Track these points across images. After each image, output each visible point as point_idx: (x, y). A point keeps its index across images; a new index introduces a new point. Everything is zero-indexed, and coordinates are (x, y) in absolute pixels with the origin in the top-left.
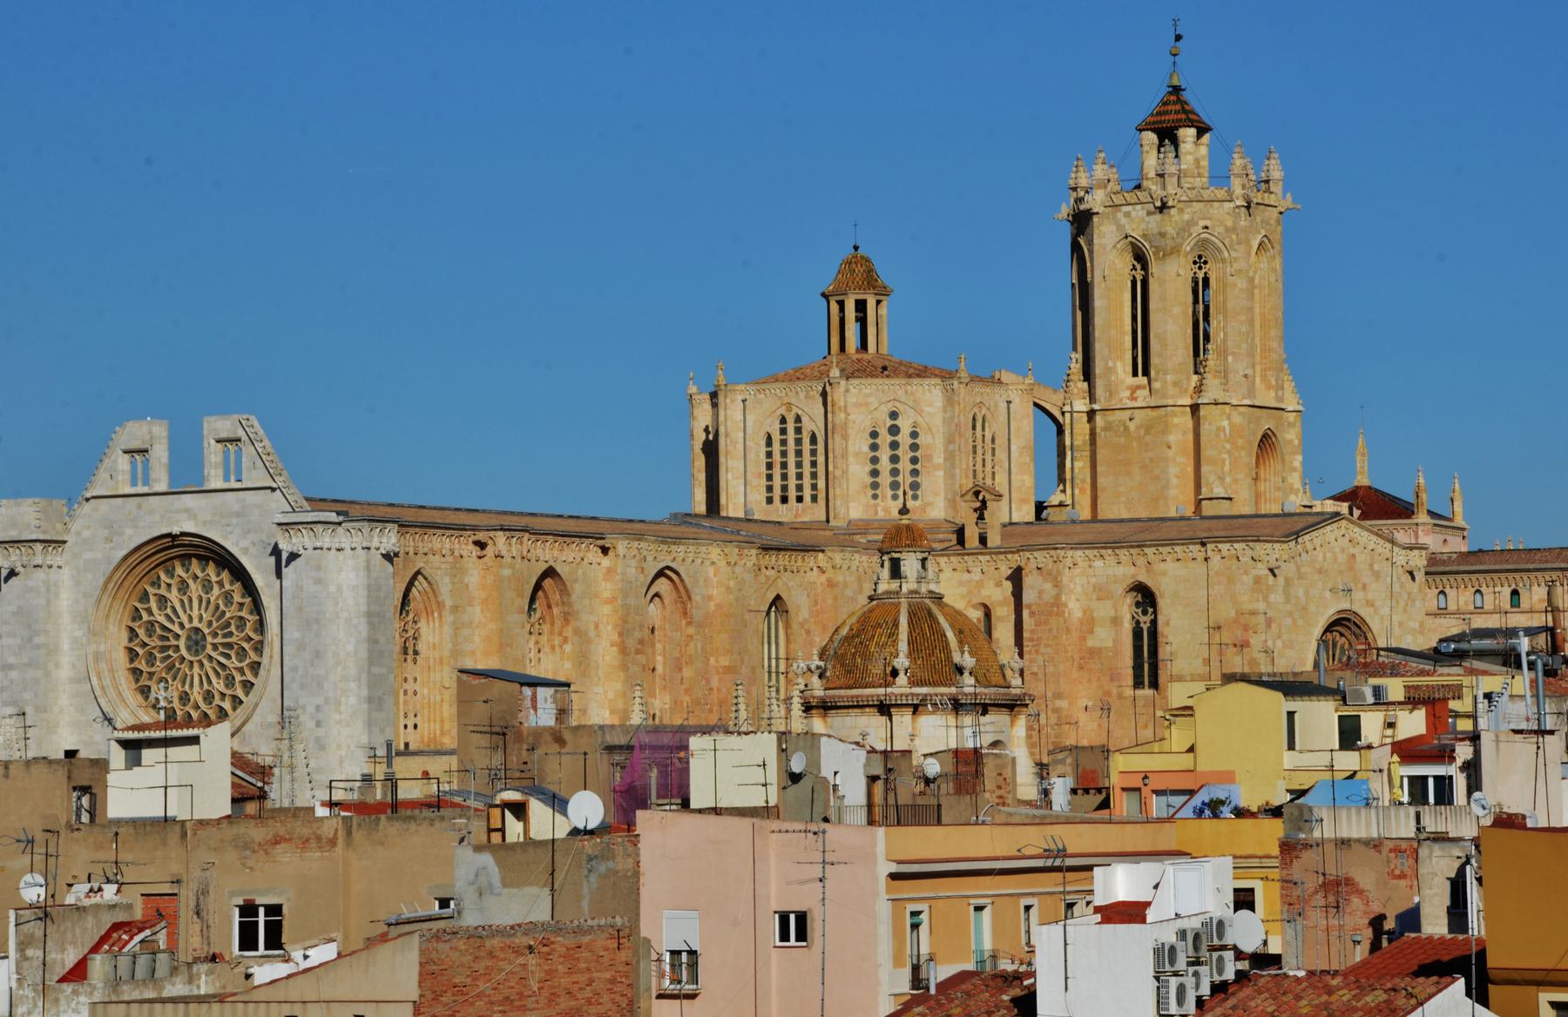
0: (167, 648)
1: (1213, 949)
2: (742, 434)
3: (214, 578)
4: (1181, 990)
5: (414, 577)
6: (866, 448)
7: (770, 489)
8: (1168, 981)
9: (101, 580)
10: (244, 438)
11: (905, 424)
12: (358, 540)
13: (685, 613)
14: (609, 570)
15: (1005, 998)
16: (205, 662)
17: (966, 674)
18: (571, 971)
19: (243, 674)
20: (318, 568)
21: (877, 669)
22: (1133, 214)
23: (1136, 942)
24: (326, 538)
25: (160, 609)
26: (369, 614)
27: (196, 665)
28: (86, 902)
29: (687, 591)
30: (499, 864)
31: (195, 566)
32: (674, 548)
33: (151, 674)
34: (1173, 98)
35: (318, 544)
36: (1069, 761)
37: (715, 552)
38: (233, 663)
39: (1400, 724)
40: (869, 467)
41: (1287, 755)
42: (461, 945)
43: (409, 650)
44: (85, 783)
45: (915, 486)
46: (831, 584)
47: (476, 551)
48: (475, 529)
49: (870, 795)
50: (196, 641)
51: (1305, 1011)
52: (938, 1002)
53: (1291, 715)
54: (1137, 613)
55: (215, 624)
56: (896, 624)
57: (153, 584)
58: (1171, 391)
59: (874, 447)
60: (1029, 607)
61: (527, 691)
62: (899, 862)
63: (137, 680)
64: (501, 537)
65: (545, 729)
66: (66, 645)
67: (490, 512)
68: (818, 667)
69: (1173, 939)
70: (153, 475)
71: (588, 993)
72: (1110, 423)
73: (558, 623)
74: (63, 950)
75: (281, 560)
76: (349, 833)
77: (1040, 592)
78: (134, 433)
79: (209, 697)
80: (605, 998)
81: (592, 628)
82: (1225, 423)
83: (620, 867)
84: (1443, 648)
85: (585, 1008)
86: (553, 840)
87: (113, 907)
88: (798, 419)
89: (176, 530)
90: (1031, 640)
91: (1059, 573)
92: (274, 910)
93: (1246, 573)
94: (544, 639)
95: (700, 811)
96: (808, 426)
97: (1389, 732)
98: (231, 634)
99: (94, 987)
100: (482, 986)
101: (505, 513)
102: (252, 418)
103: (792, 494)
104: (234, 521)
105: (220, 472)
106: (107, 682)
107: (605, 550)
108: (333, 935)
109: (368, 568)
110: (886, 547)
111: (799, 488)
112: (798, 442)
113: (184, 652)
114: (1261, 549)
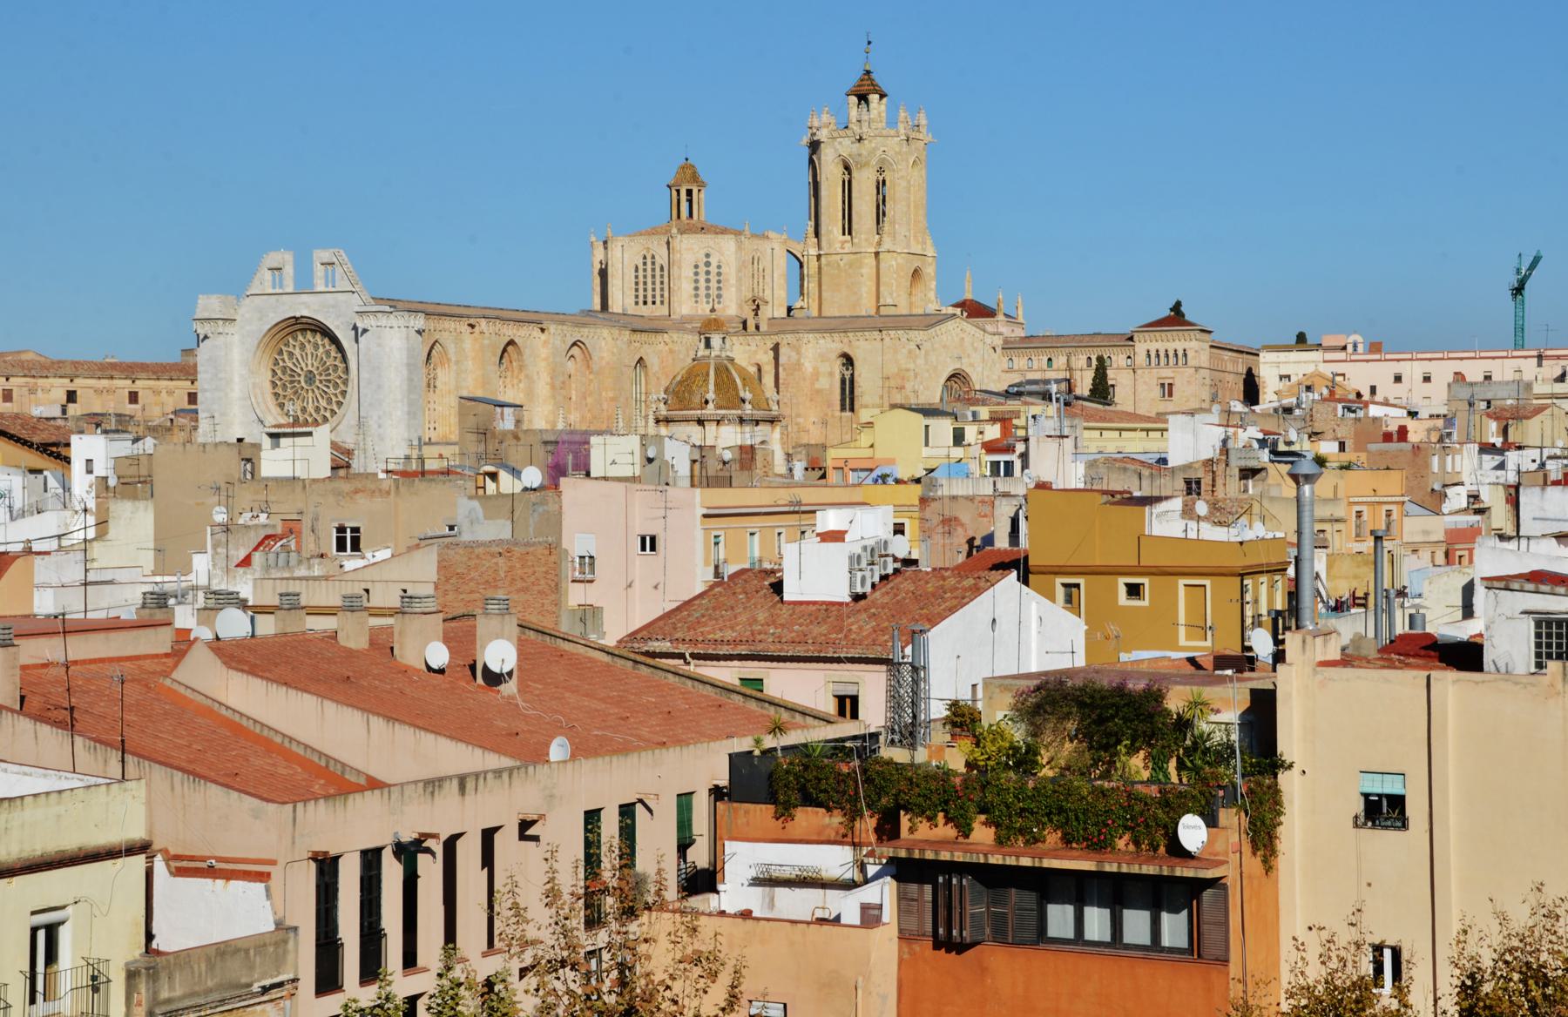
0: (294, 381)
1: (881, 556)
3: (320, 343)
4: (863, 580)
5: (434, 344)
6: (692, 274)
7: (637, 297)
9: (256, 342)
10: (337, 262)
11: (714, 261)
12: (402, 322)
13: (588, 367)
14: (545, 342)
15: (766, 583)
17: (747, 403)
20: (379, 338)
21: (697, 400)
23: (838, 555)
24: (383, 320)
26: (408, 365)
28: (250, 523)
29: (590, 355)
30: (481, 504)
32: (582, 329)
33: (285, 396)
34: (866, 77)
37: (605, 332)
38: (331, 391)
39: (986, 432)
40: (693, 285)
42: (461, 551)
43: (431, 385)
44: (248, 457)
45: (719, 296)
46: (671, 351)
48: (469, 317)
49: (692, 470)
50: (310, 378)
51: (930, 590)
52: (729, 585)
53: (927, 427)
55: (321, 369)
56: (708, 375)
57: (285, 345)
58: (864, 244)
59: (696, 274)
61: (498, 410)
62: (708, 508)
64: (483, 322)
65: (508, 431)
66: (236, 379)
67: (477, 307)
69: (859, 551)
70: (285, 283)
71: (532, 579)
74: (237, 549)
75: (358, 332)
76: (397, 488)
77: (789, 357)
78: (273, 259)
79: (317, 409)
80: (542, 582)
82: (894, 263)
84: (1011, 390)
87: (266, 526)
88: (653, 257)
89: (298, 315)
91: (800, 346)
92: (356, 530)
94: (508, 380)
95: (596, 478)
96: (659, 261)
97: (980, 436)
98: (330, 374)
99: (255, 570)
100: (473, 574)
101: (486, 308)
102: (342, 252)
103: (650, 300)
105: (323, 281)
106: (260, 400)
107: (543, 330)
109: (407, 338)
110: (703, 331)
111: (654, 296)
112: (653, 270)
113: (303, 384)
114: (912, 334)
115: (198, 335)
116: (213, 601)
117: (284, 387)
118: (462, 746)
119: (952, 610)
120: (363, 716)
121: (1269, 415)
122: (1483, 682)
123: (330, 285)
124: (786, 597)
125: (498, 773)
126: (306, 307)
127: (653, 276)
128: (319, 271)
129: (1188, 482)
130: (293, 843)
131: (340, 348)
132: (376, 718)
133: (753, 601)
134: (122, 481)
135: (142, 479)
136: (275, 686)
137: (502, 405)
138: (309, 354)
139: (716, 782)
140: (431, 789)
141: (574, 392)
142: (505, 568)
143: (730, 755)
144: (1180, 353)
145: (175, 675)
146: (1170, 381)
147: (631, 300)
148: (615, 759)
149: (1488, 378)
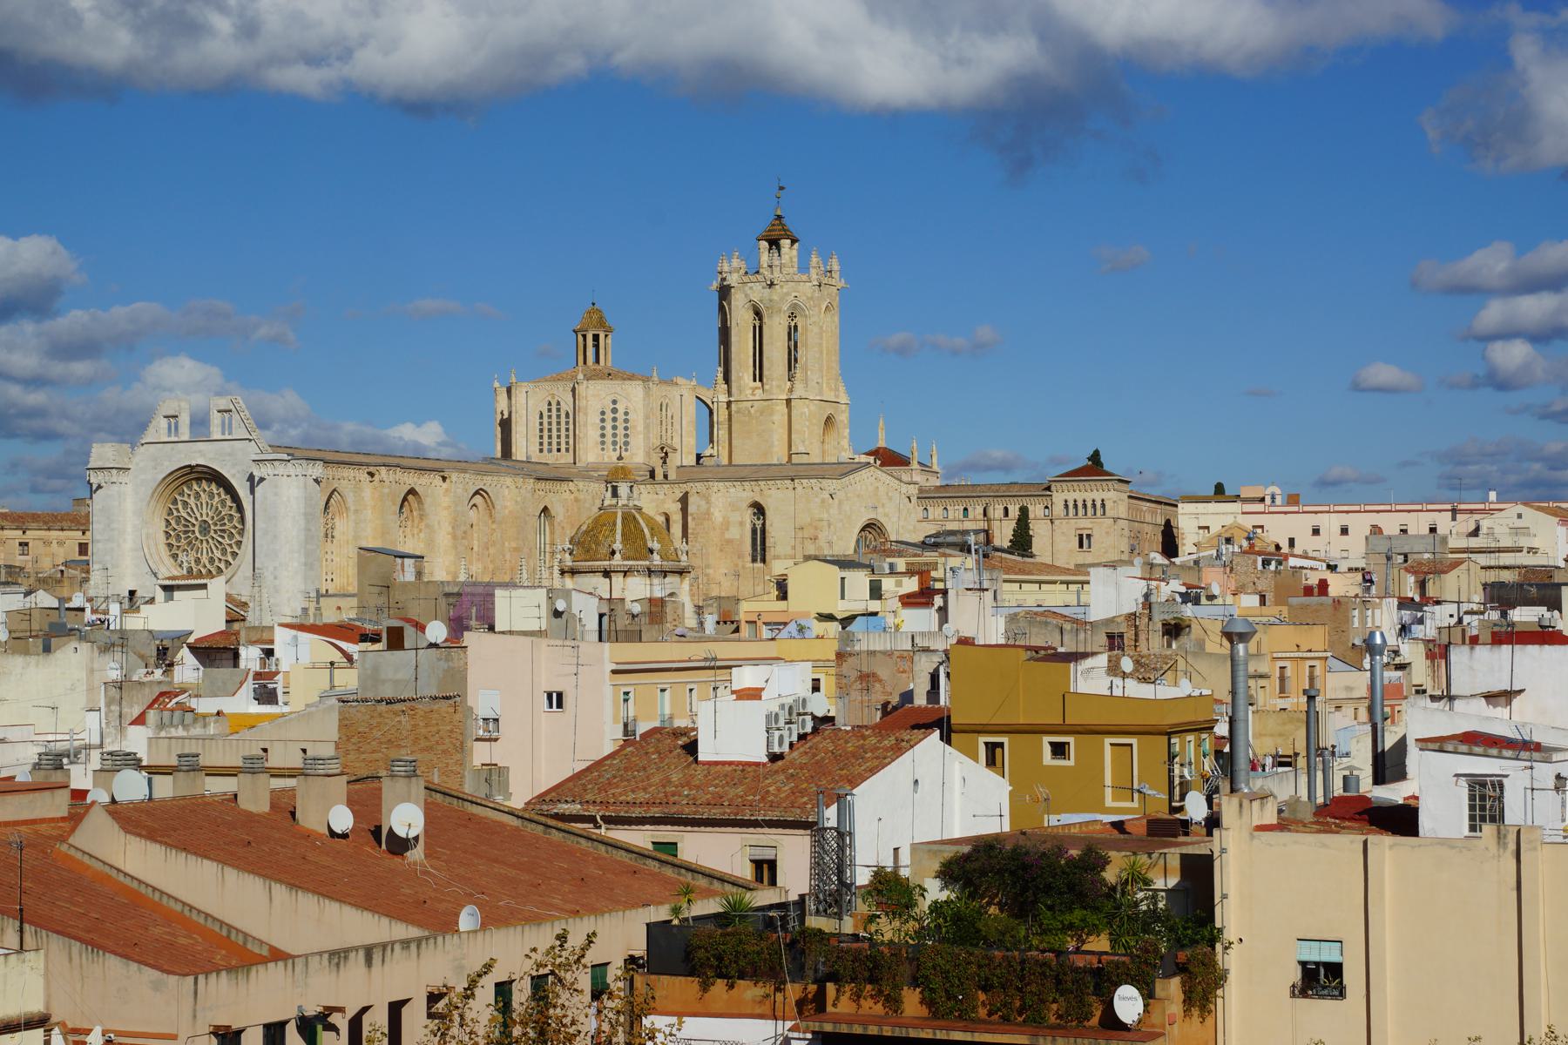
0: (188, 532)
1: (799, 714)
3: (215, 492)
4: (781, 738)
5: (332, 493)
6: (598, 421)
9: (150, 492)
10: (234, 409)
11: (621, 407)
12: (299, 470)
14: (447, 490)
16: (210, 540)
17: (655, 554)
18: (427, 725)
19: (232, 548)
23: (755, 713)
24: (281, 469)
26: (305, 514)
28: (145, 680)
31: (204, 485)
32: (485, 478)
35: (276, 473)
36: (715, 605)
37: (509, 481)
38: (226, 541)
40: (600, 432)
41: (840, 602)
43: (329, 535)
45: (626, 443)
46: (577, 500)
47: (368, 478)
48: (368, 465)
50: (205, 527)
53: (843, 579)
57: (180, 494)
58: (775, 391)
59: (603, 420)
60: (692, 515)
61: (399, 561)
62: (617, 663)
66: (129, 529)
69: (777, 709)
70: (180, 431)
73: (416, 521)
74: (132, 707)
77: (699, 506)
79: (212, 561)
81: (436, 523)
83: (456, 665)
87: (160, 683)
88: (558, 403)
89: (194, 463)
90: (693, 534)
94: (408, 530)
95: (503, 633)
96: (564, 407)
98: (225, 524)
102: (239, 398)
104: (228, 458)
105: (220, 429)
107: (444, 479)
109: (305, 487)
110: (609, 479)
111: (559, 444)
112: (558, 417)
113: (197, 534)
115: (91, 485)
116: (110, 762)
117: (178, 538)
118: (367, 915)
119: (873, 771)
120: (265, 884)
121: (1190, 568)
122: (1420, 846)
124: (701, 758)
125: (405, 944)
127: (559, 423)
129: (1111, 637)
130: (195, 1017)
131: (235, 498)
132: (278, 885)
133: (667, 761)
134: (14, 635)
135: (33, 634)
137: (402, 557)
138: (204, 503)
139: (631, 953)
140: (336, 960)
141: (475, 542)
142: (409, 728)
143: (647, 924)
144: (1098, 504)
145: (71, 840)
146: (1089, 532)
148: (527, 928)
149: (1404, 531)
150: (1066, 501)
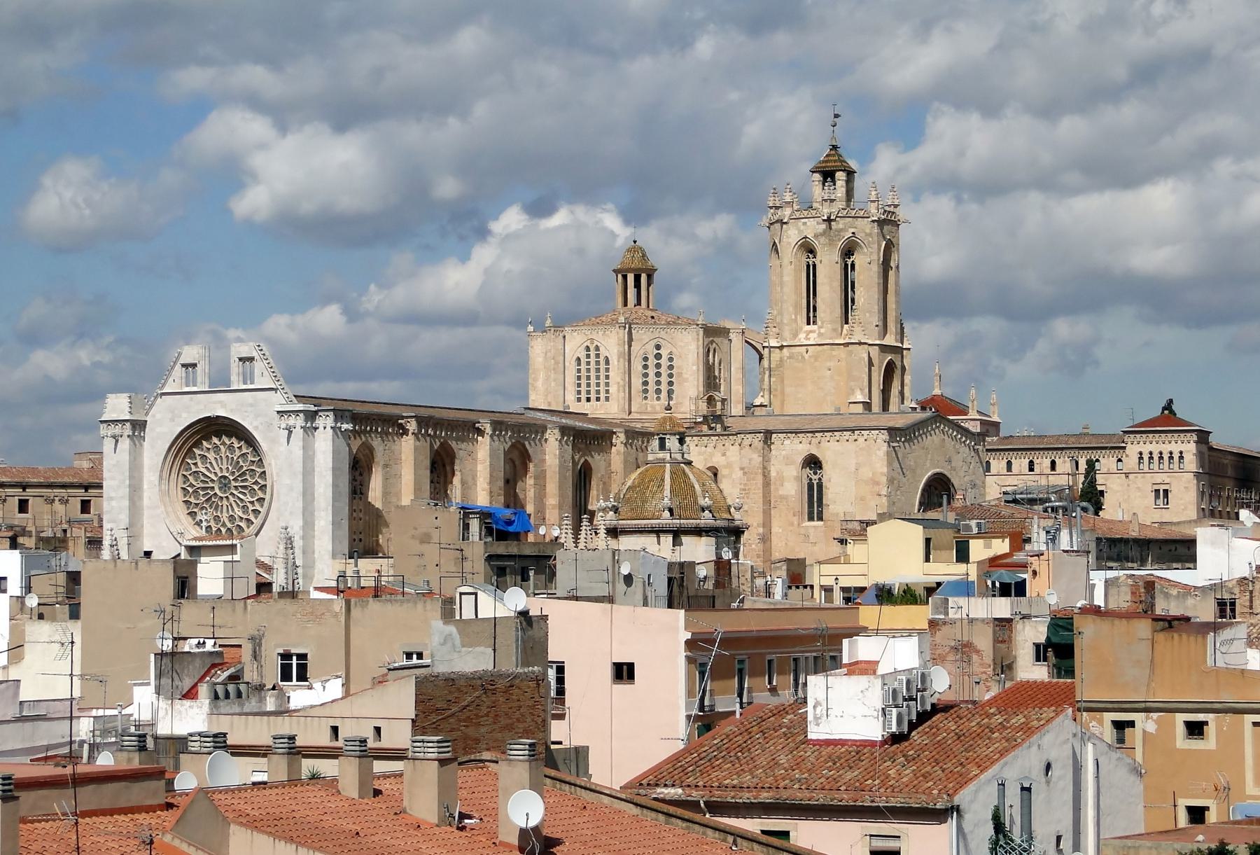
0: (207, 488)
2: (562, 358)
7: (579, 392)
8: (891, 711)
11: (664, 352)
19: (254, 506)
22: (808, 224)
25: (202, 463)
27: (224, 499)
34: (833, 152)
50: (224, 482)
54: (810, 473)
56: (663, 480)
59: (646, 367)
63: (188, 508)
68: (614, 506)
71: (517, 715)
72: (793, 353)
77: (750, 460)
78: (190, 353)
79: (232, 518)
80: (529, 720)
85: (516, 724)
86: (495, 618)
88: (597, 348)
92: (302, 657)
93: (879, 450)
96: (603, 352)
98: (246, 480)
103: (593, 396)
104: (250, 409)
108: (339, 674)
111: (598, 392)
112: (598, 363)
113: (217, 491)
123: (249, 382)
126: (220, 406)
127: (598, 370)
128: (235, 367)
136: (283, 843)
144: (1176, 456)
146: (1166, 487)
147: (571, 397)
150: (1141, 453)
